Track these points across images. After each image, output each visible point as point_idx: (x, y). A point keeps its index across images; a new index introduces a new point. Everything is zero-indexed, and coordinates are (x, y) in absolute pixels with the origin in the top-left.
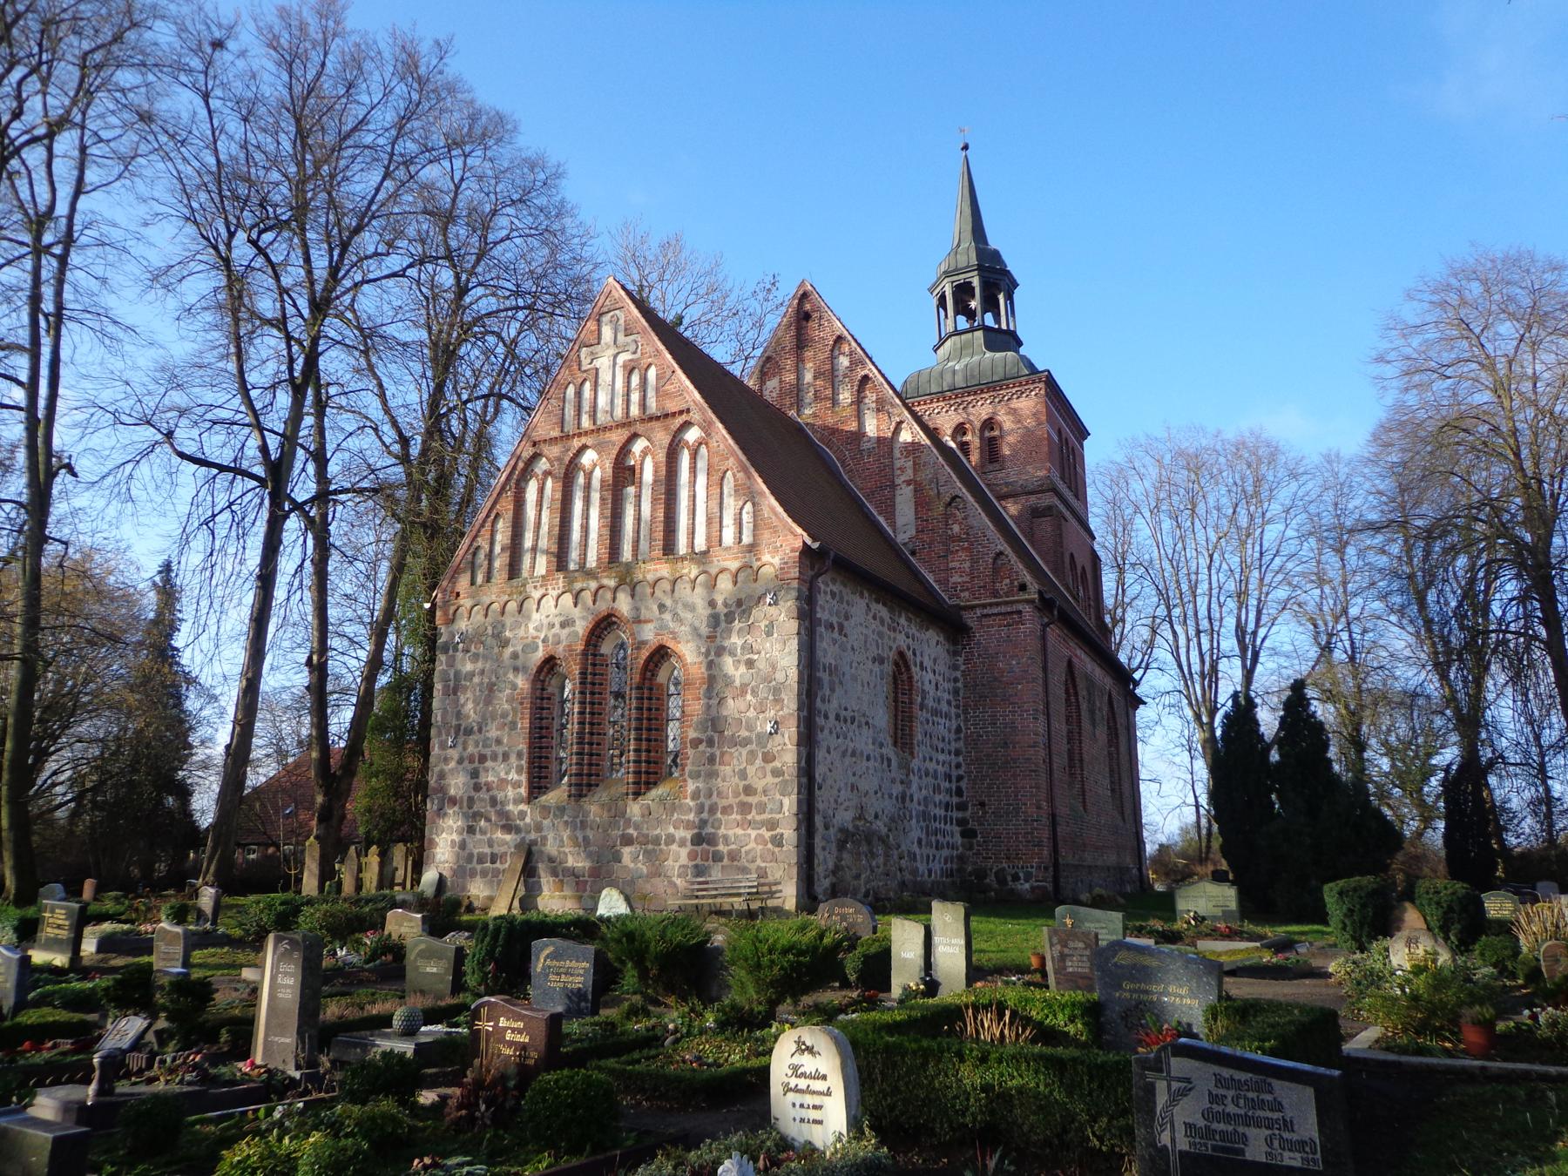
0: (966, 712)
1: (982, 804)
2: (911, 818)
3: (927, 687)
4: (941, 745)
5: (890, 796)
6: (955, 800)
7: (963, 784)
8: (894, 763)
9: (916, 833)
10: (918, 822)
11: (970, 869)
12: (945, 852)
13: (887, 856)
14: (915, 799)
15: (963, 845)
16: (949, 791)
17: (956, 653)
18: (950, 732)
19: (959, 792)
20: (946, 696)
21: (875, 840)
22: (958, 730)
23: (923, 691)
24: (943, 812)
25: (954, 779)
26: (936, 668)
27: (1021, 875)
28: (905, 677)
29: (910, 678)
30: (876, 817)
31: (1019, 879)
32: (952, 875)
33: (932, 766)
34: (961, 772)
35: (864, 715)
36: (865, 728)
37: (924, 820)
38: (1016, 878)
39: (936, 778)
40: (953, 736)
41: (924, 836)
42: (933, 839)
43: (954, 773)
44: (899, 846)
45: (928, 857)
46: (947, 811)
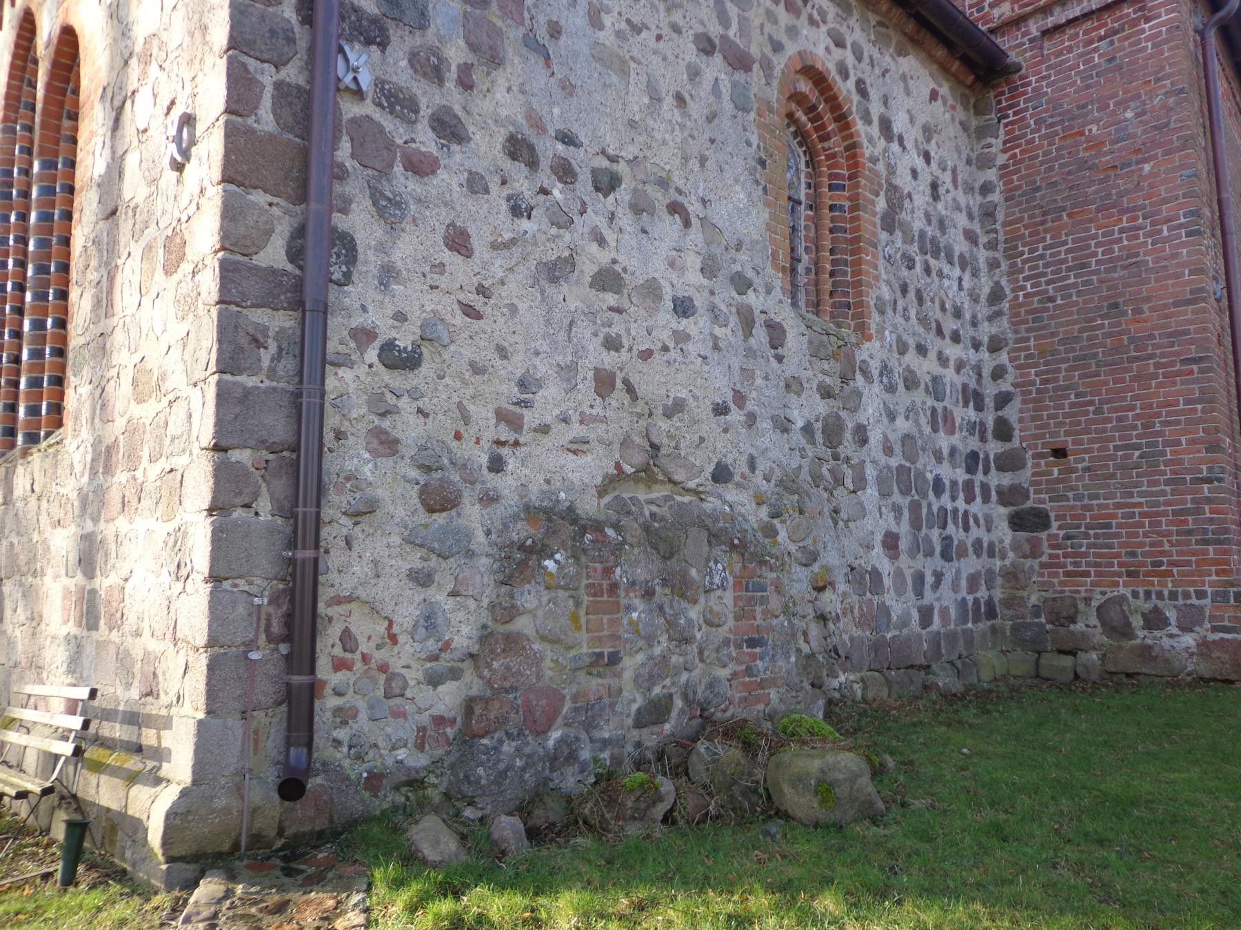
0: (1011, 252)
1: (1060, 453)
2: (860, 482)
3: (903, 180)
4: (950, 325)
5: (783, 426)
6: (994, 448)
7: (1012, 412)
8: (795, 341)
9: (877, 523)
10: (885, 494)
11: (1034, 599)
12: (971, 564)
13: (749, 588)
14: (875, 437)
15: (1016, 547)
16: (977, 429)
17: (981, 133)
18: (975, 299)
19: (1003, 431)
20: (962, 220)
21: (695, 545)
22: (996, 296)
23: (893, 188)
24: (961, 475)
25: (989, 402)
26: (932, 148)
27: (1172, 615)
28: (836, 144)
29: (852, 148)
30: (721, 474)
31: (1165, 623)
32: (991, 614)
33: (926, 367)
34: (1005, 386)
35: (663, 183)
36: (669, 227)
37: (905, 492)
38: (1155, 620)
39: (939, 397)
40: (983, 310)
41: (904, 528)
42: (935, 535)
43: (990, 390)
44: (811, 558)
45: (919, 578)
46: (971, 470)
